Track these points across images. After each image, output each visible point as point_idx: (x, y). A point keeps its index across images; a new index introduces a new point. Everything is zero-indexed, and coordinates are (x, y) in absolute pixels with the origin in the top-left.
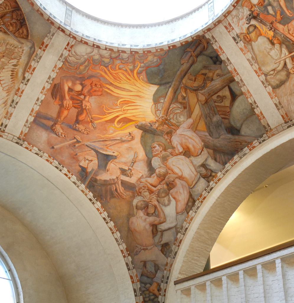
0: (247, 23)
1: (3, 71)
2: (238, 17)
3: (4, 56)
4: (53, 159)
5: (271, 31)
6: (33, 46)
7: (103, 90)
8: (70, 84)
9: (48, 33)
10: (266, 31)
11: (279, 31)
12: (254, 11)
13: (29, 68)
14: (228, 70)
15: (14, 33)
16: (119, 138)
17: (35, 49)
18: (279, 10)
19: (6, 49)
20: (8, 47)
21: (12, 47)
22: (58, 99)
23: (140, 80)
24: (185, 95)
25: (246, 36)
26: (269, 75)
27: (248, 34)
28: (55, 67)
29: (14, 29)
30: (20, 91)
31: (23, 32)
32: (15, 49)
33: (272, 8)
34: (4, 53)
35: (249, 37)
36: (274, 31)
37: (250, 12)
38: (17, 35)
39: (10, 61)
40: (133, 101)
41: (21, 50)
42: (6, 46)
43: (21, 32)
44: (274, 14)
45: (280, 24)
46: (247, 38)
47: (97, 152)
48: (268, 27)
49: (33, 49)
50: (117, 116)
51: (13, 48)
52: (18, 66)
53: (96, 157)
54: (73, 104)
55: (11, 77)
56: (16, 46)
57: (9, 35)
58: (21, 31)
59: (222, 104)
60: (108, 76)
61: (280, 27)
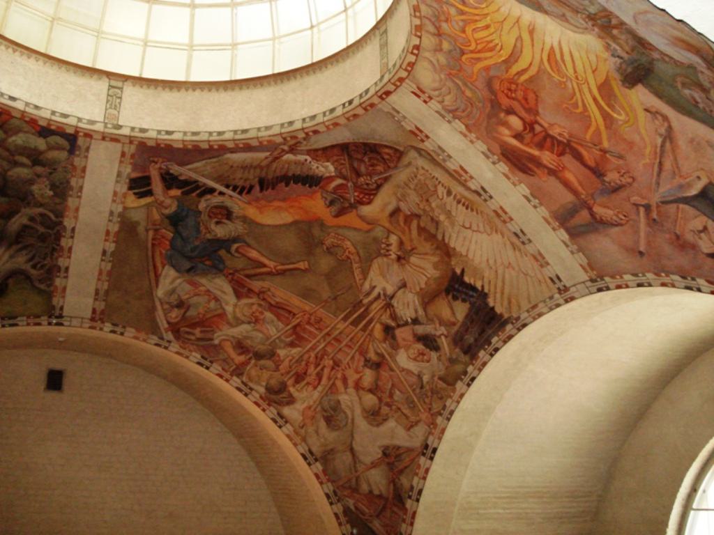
1: (454, 214)
3: (427, 201)
4: (667, 276)
6: (418, 150)
7: (522, 85)
9: (393, 115)
13: (461, 176)
15: (389, 167)
16: (659, 141)
19: (415, 190)
20: (412, 187)
22: (535, 169)
28: (465, 136)
29: (381, 164)
30: (500, 212)
31: (388, 154)
39: (438, 196)
41: (421, 172)
42: (410, 188)
47: (686, 200)
49: (423, 153)
52: (453, 190)
53: (698, 213)
55: (469, 209)
56: (413, 175)
57: (390, 176)
58: (386, 157)
60: (486, 59)
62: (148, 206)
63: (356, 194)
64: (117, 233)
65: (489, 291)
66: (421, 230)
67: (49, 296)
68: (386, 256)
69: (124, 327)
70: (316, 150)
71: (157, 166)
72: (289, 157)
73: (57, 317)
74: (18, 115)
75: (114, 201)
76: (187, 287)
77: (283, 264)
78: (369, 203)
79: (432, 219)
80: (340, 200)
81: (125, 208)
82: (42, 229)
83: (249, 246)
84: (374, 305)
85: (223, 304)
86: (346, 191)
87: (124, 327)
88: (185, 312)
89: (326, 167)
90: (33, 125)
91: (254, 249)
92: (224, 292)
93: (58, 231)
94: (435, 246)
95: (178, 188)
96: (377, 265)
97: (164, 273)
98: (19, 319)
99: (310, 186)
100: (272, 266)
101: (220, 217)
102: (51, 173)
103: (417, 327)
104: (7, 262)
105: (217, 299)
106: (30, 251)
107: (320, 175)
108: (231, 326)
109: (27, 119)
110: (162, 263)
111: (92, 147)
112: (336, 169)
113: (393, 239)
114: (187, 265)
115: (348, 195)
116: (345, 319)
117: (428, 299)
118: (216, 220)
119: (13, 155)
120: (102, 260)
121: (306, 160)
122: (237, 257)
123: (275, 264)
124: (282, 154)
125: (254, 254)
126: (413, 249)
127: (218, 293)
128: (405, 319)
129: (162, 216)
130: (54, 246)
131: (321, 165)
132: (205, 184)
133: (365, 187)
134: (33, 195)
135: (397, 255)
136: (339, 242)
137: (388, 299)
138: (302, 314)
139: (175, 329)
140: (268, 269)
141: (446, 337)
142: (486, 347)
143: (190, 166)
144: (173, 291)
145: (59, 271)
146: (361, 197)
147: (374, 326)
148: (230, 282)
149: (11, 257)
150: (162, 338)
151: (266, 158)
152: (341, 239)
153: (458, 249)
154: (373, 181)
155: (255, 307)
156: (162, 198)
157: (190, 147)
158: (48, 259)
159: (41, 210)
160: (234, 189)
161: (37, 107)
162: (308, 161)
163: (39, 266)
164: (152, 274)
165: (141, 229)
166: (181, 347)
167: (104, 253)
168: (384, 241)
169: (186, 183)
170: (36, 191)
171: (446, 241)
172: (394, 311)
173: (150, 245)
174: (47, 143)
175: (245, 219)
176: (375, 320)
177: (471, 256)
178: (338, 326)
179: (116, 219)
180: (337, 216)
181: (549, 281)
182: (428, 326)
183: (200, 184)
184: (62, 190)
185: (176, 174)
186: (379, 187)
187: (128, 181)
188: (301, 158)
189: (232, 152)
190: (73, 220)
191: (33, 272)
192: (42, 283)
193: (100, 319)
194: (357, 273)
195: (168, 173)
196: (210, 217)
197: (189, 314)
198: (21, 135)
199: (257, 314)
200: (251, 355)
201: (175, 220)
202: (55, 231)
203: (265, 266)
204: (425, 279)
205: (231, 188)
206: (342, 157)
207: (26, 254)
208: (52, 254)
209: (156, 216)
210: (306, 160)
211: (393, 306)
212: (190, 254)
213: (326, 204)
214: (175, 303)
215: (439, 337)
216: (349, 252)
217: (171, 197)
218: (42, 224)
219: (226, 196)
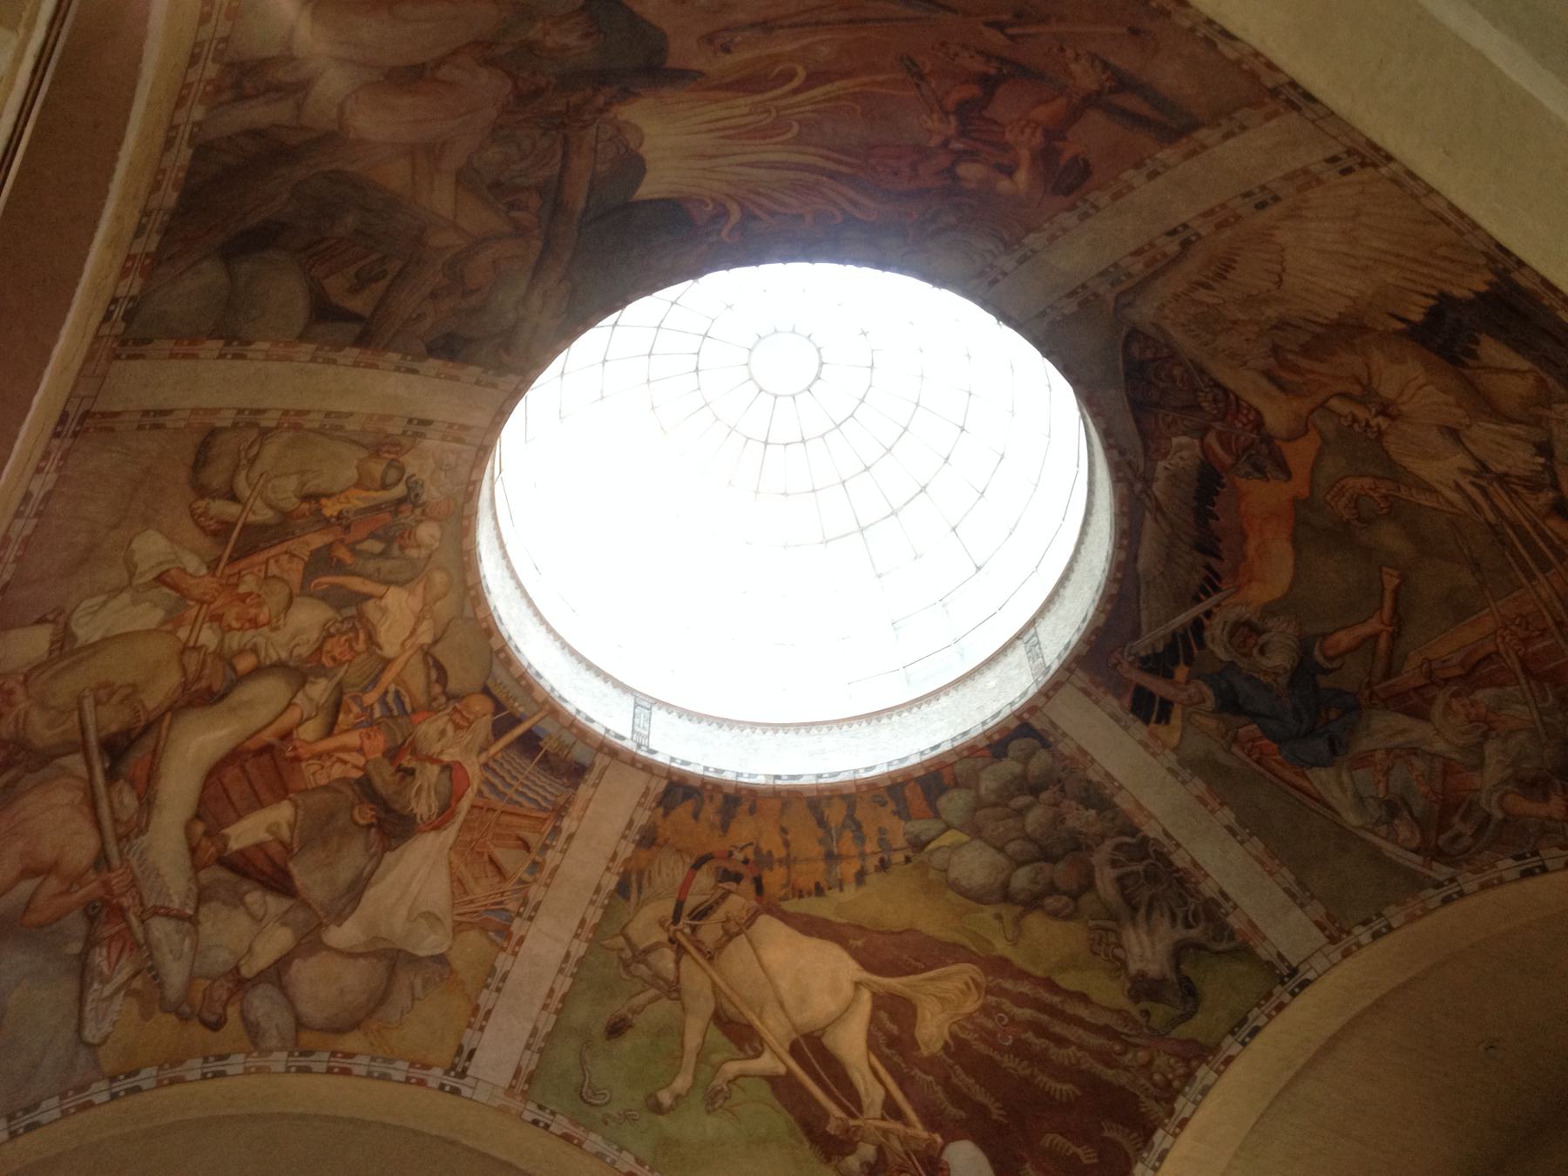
0: (414, 475)
1: (1255, 292)
2: (446, 471)
5: (335, 514)
8: (1004, 185)
10: (349, 502)
11: (315, 531)
12: (412, 511)
14: (395, 350)
18: (350, 565)
23: (713, 200)
24: (515, 214)
25: (397, 453)
26: (255, 440)
27: (393, 460)
33: (372, 553)
35: (386, 455)
36: (328, 520)
37: (420, 502)
38: (1166, 350)
40: (729, 141)
44: (359, 547)
45: (325, 546)
46: (389, 452)
48: (350, 515)
50: (795, 92)
51: (1193, 327)
54: (1003, 133)
55: (1234, 265)
57: (1191, 361)
58: (1149, 354)
59: (352, 270)
61: (317, 540)
65: (1433, 287)
66: (1306, 351)
67: (1244, 952)
68: (1381, 433)
69: (1379, 915)
70: (1146, 448)
71: (1126, 665)
72: (1158, 488)
74: (955, 758)
75: (1154, 755)
77: (1381, 608)
78: (1258, 413)
80: (1251, 455)
81: (1175, 750)
83: (1324, 636)
84: (1502, 506)
85: (1425, 748)
86: (1234, 437)
87: (1379, 915)
88: (1411, 813)
89: (1181, 447)
90: (979, 754)
91: (1336, 630)
92: (1403, 732)
93: (1155, 851)
95: (1176, 663)
98: (1251, 1017)
99: (1223, 486)
100: (1381, 627)
101: (1251, 642)
102: (1062, 790)
104: (1153, 943)
105: (1414, 751)
107: (1198, 462)
108: (1480, 766)
109: (966, 753)
110: (1297, 774)
111: (1054, 718)
112: (1185, 434)
116: (1531, 577)
117: (1486, 406)
118: (1255, 651)
120: (1242, 843)
124: (1150, 492)
125: (1344, 639)
127: (1400, 740)
128: (1540, 469)
133: (1221, 405)
134: (1080, 833)
137: (1488, 475)
138: (1499, 640)
139: (1436, 854)
140: (1384, 636)
143: (1144, 627)
144: (1360, 799)
145: (1219, 906)
146: (1245, 420)
147: (1557, 535)
149: (1151, 932)
150: (1438, 885)
151: (1156, 520)
154: (1208, 390)
155: (1456, 705)
156: (1184, 696)
157: (1109, 607)
158: (1190, 900)
159: (1108, 844)
160: (1208, 595)
161: (964, 734)
162: (1169, 466)
164: (1317, 806)
165: (1222, 758)
166: (1474, 872)
167: (1230, 829)
169: (1171, 647)
171: (1325, 322)
172: (1518, 477)
173: (1255, 765)
174: (1013, 759)
175: (1269, 610)
176: (1539, 521)
177: (1352, 293)
178: (1544, 595)
179: (1186, 774)
180: (1289, 475)
181: (1345, 179)
184: (1097, 797)
186: (1217, 385)
187: (1131, 716)
189: (1136, 558)
190: (1152, 822)
191: (1194, 933)
193: (1341, 930)
194: (1425, 500)
195: (1145, 660)
196: (1245, 655)
197: (1417, 810)
198: (984, 775)
200: (1558, 783)
201: (1230, 704)
203: (1375, 637)
205: (1202, 596)
207: (1162, 915)
209: (1211, 723)
210: (1166, 468)
211: (1506, 475)
213: (1260, 479)
214: (1384, 813)
217: (1188, 682)
218: (1131, 860)
219: (1215, 610)
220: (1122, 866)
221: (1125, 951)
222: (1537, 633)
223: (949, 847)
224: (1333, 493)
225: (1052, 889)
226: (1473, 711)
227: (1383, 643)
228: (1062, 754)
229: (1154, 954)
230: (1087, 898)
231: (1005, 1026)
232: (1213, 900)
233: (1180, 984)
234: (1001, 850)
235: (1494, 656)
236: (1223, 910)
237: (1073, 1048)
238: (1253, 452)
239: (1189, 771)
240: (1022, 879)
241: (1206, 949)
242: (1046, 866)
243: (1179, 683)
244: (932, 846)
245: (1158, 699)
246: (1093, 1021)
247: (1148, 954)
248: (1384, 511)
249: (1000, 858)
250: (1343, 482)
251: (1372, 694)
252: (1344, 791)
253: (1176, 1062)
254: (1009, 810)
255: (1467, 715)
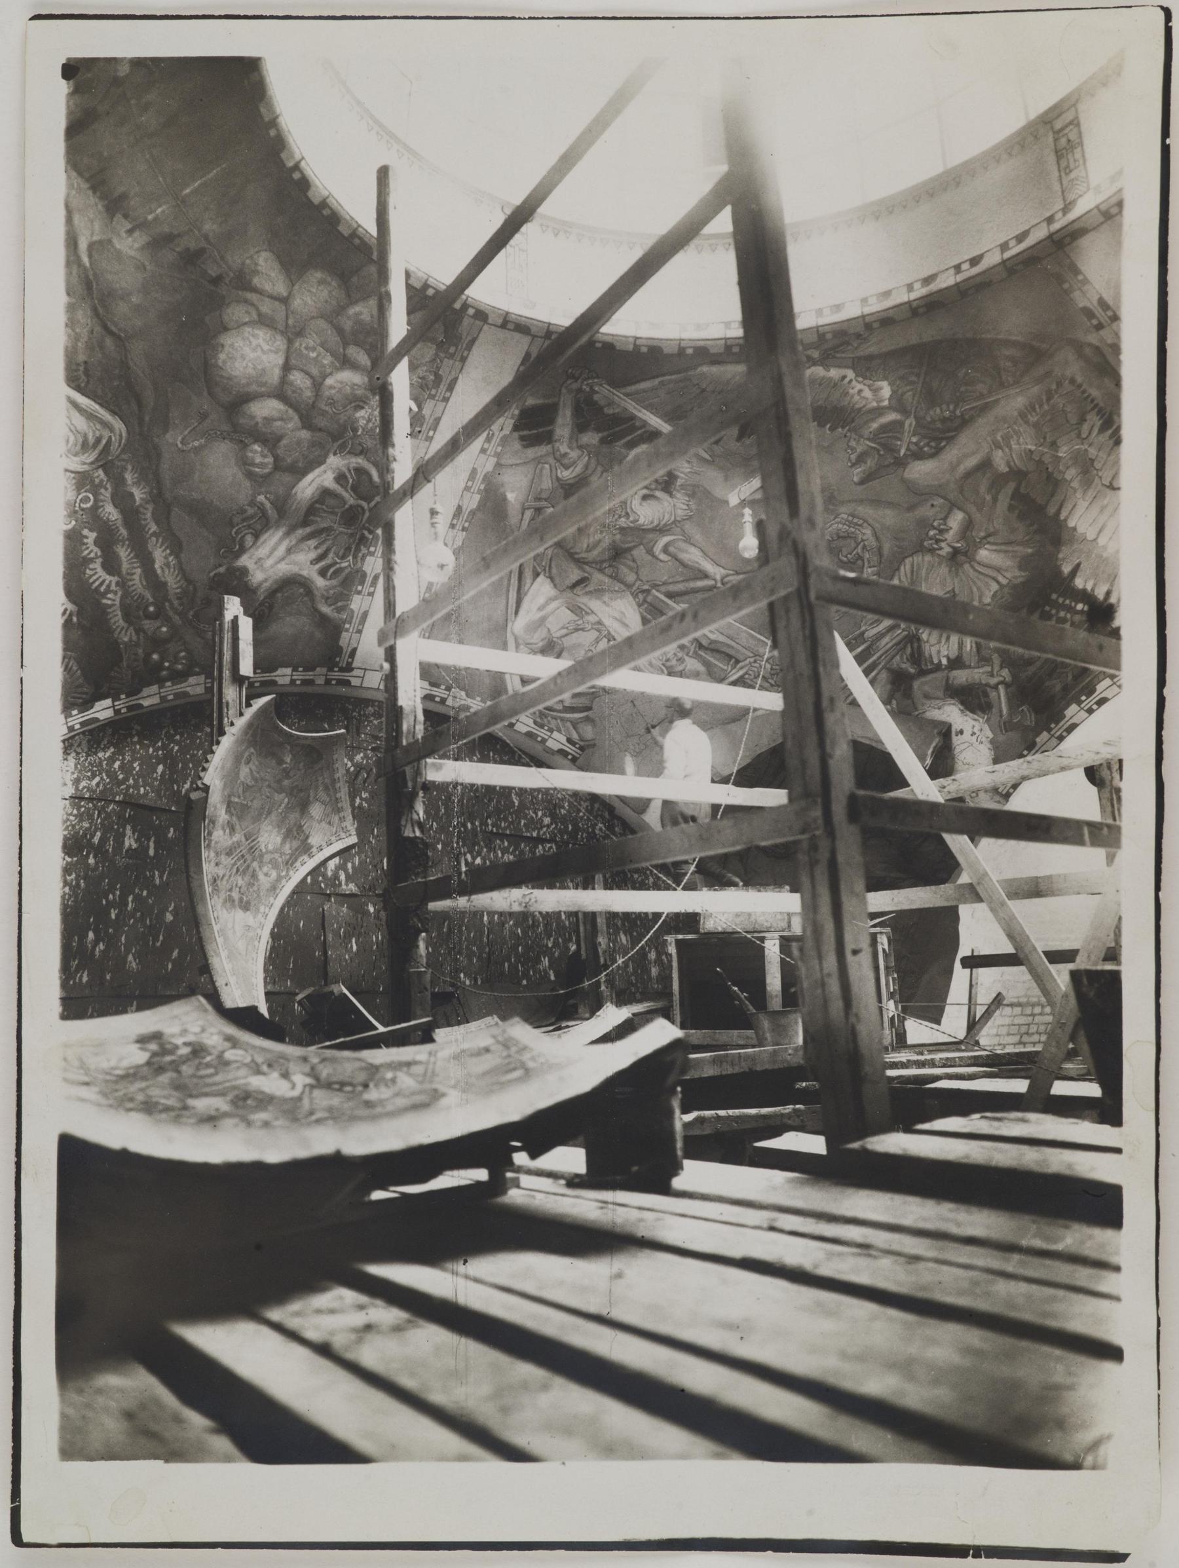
1: (1098, 465)
17: (1090, 345)
19: (1036, 426)
21: (1041, 406)
32: (1052, 402)
34: (1045, 438)
43: (1008, 364)
51: (1046, 407)
57: (997, 401)
62: (538, 461)
63: (914, 440)
64: (473, 513)
68: (931, 551)
71: (575, 386)
73: (342, 670)
76: (566, 616)
78: (932, 456)
79: (1050, 476)
81: (498, 465)
82: (350, 499)
86: (899, 436)
87: (448, 689)
89: (876, 391)
94: (1035, 527)
96: (908, 567)
97: (531, 591)
99: (832, 429)
100: (718, 577)
103: (955, 673)
104: (283, 559)
106: (323, 542)
107: (857, 406)
112: (894, 392)
113: (956, 520)
114: (575, 575)
115: (899, 443)
119: (345, 344)
121: (844, 377)
122: (661, 561)
123: (723, 572)
126: (989, 535)
128: (936, 661)
129: (556, 484)
130: (366, 533)
131: (869, 386)
132: (645, 424)
133: (939, 425)
134: (355, 430)
135: (953, 547)
136: (853, 530)
141: (1007, 686)
142: (1083, 698)
143: (630, 389)
145: (362, 583)
146: (922, 444)
148: (639, 605)
149: (289, 551)
152: (856, 524)
153: (1081, 529)
156: (564, 448)
157: (644, 350)
158: (351, 558)
162: (847, 380)
163: (332, 570)
164: (513, 595)
166: (535, 723)
168: (935, 524)
170: (362, 422)
172: (919, 647)
177: (1102, 541)
179: (479, 485)
182: (976, 670)
183: (637, 424)
185: (602, 403)
188: (834, 373)
191: (320, 582)
192: (330, 605)
199: (674, 662)
202: (373, 504)
203: (706, 576)
204: (995, 587)
206: (916, 370)
207: (316, 548)
208: (358, 549)
210: (844, 377)
212: (583, 555)
214: (541, 644)
215: (996, 687)
216: (864, 547)
217: (580, 447)
220: (342, 486)
221: (254, 544)
222: (773, 683)
223: (260, 314)
224: (850, 518)
225: (270, 441)
226: (674, 662)
227: (700, 584)
228: (438, 368)
229: (272, 567)
230: (287, 478)
231: (83, 509)
232: (364, 575)
233: (260, 605)
234: (287, 367)
235: (733, 660)
236: (360, 588)
237: (114, 579)
238: (882, 453)
239: (482, 487)
240: (265, 409)
241: (313, 600)
242: (295, 421)
243: (577, 441)
244: (249, 295)
245: (549, 428)
246: (159, 571)
247: (269, 562)
248: (845, 559)
249: (277, 373)
250: (865, 525)
251: (648, 591)
252: (541, 609)
253: (184, 658)
254: (341, 350)
255: (668, 660)
